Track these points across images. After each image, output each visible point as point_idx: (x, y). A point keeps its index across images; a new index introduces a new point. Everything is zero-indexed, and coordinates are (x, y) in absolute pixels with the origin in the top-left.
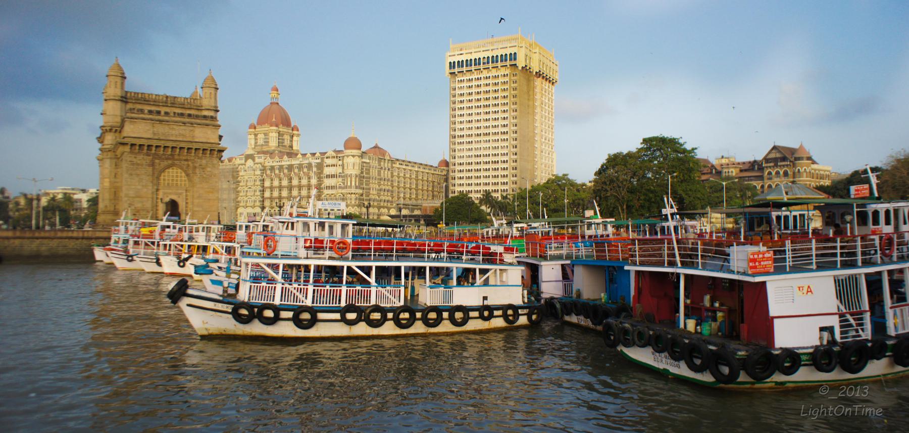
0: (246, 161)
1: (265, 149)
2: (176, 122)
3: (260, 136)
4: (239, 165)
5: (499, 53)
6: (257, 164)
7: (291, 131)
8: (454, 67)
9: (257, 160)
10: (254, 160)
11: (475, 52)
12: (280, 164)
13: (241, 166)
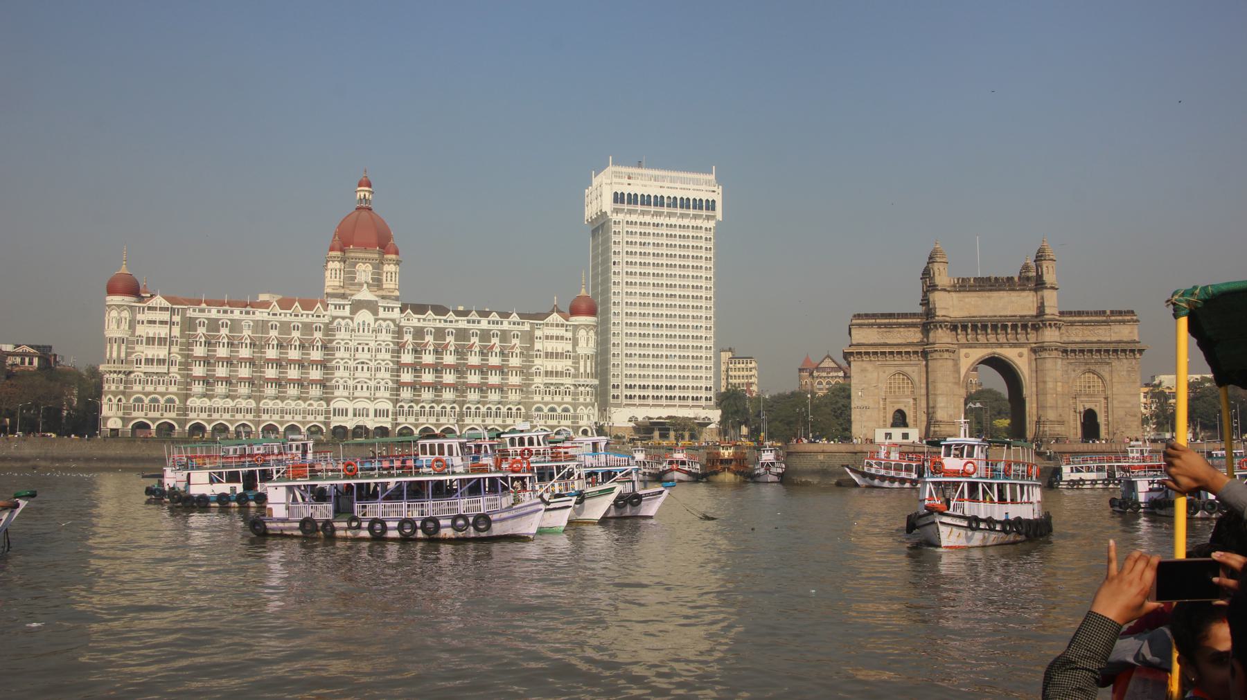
3: (361, 267)
4: (335, 318)
6: (384, 320)
9: (382, 314)
10: (375, 312)
12: (438, 325)
13: (339, 320)
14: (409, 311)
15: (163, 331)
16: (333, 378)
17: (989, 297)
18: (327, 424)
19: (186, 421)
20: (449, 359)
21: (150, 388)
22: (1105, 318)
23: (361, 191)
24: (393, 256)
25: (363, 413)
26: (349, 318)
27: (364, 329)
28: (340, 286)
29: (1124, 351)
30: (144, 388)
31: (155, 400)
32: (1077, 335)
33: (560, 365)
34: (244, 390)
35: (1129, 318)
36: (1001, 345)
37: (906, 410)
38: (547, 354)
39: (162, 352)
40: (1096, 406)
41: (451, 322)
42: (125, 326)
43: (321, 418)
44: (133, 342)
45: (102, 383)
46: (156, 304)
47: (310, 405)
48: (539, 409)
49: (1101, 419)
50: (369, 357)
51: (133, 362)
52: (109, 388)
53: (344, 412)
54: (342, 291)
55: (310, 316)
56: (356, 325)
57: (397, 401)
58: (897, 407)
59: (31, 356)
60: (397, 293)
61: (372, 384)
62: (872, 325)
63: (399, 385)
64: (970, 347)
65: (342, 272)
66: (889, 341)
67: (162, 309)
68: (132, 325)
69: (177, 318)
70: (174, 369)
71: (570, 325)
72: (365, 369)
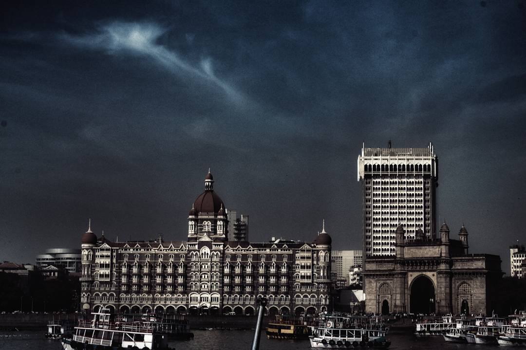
0: (200, 247)
4: (189, 251)
8: (370, 170)
9: (214, 247)
10: (210, 247)
12: (243, 252)
13: (193, 252)
14: (228, 246)
15: (108, 261)
17: (421, 249)
18: (187, 305)
19: (119, 305)
21: (102, 289)
23: (207, 182)
24: (222, 217)
25: (206, 299)
26: (196, 250)
29: (477, 273)
30: (99, 289)
32: (459, 266)
33: (308, 272)
34: (145, 289)
36: (425, 271)
37: (388, 300)
38: (302, 266)
39: (107, 271)
43: (184, 303)
44: (94, 266)
48: (298, 296)
49: (469, 305)
51: (94, 276)
53: (196, 299)
54: (195, 236)
57: (223, 293)
58: (384, 299)
59: (54, 271)
60: (224, 236)
61: (209, 284)
62: (373, 262)
63: (223, 284)
64: (412, 272)
68: (94, 257)
71: (315, 250)
72: (206, 276)
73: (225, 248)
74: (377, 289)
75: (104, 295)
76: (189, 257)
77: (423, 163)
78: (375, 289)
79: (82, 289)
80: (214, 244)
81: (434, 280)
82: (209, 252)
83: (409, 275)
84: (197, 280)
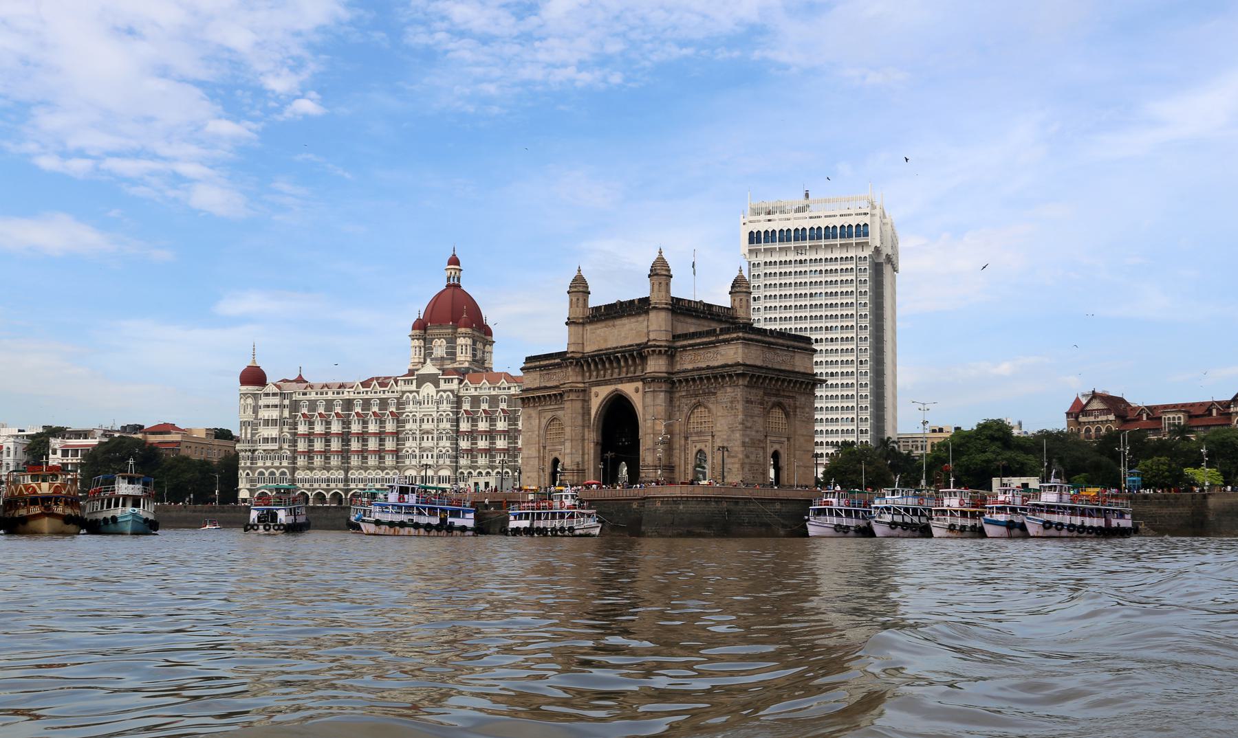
0: (419, 386)
1: (449, 366)
2: (783, 345)
3: (437, 342)
4: (404, 393)
5: (838, 222)
6: (445, 391)
7: (483, 336)
9: (443, 386)
10: (437, 385)
11: (795, 219)
12: (493, 393)
13: (408, 394)
14: (466, 381)
15: (275, 414)
16: (404, 448)
20: (501, 425)
21: (268, 463)
22: (714, 338)
27: (428, 401)
28: (419, 362)
30: (264, 463)
31: (272, 473)
32: (690, 362)
34: (335, 461)
35: (734, 335)
36: (621, 381)
39: (273, 432)
40: (706, 446)
41: (504, 389)
42: (250, 411)
44: (256, 425)
45: (238, 461)
46: (270, 390)
47: (387, 474)
50: (432, 427)
52: (245, 464)
55: (386, 392)
56: (421, 398)
63: (457, 454)
65: (422, 349)
66: (548, 385)
67: (274, 394)
68: (256, 409)
69: (287, 402)
70: (286, 446)
73: (461, 386)
74: (542, 432)
75: (272, 473)
76: (403, 404)
77: (853, 221)
78: (537, 433)
79: (243, 465)
80: (442, 379)
81: (637, 401)
82: (435, 395)
83: (593, 394)
84: (415, 445)
